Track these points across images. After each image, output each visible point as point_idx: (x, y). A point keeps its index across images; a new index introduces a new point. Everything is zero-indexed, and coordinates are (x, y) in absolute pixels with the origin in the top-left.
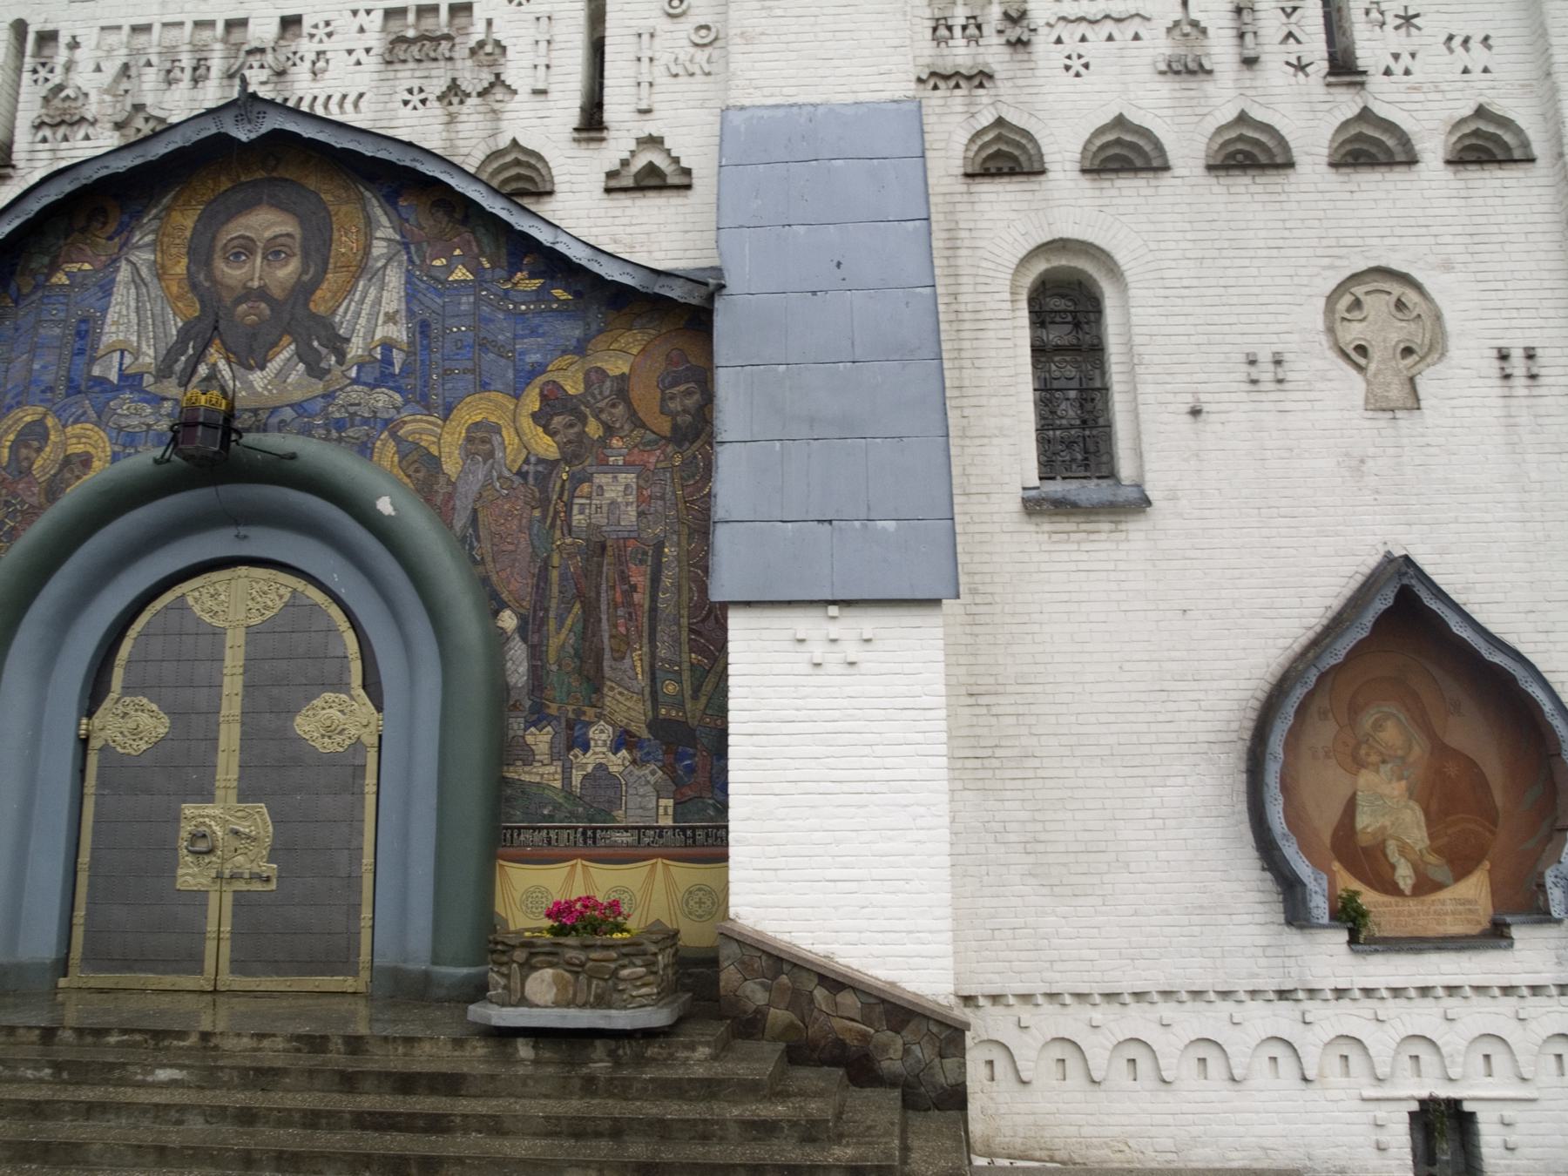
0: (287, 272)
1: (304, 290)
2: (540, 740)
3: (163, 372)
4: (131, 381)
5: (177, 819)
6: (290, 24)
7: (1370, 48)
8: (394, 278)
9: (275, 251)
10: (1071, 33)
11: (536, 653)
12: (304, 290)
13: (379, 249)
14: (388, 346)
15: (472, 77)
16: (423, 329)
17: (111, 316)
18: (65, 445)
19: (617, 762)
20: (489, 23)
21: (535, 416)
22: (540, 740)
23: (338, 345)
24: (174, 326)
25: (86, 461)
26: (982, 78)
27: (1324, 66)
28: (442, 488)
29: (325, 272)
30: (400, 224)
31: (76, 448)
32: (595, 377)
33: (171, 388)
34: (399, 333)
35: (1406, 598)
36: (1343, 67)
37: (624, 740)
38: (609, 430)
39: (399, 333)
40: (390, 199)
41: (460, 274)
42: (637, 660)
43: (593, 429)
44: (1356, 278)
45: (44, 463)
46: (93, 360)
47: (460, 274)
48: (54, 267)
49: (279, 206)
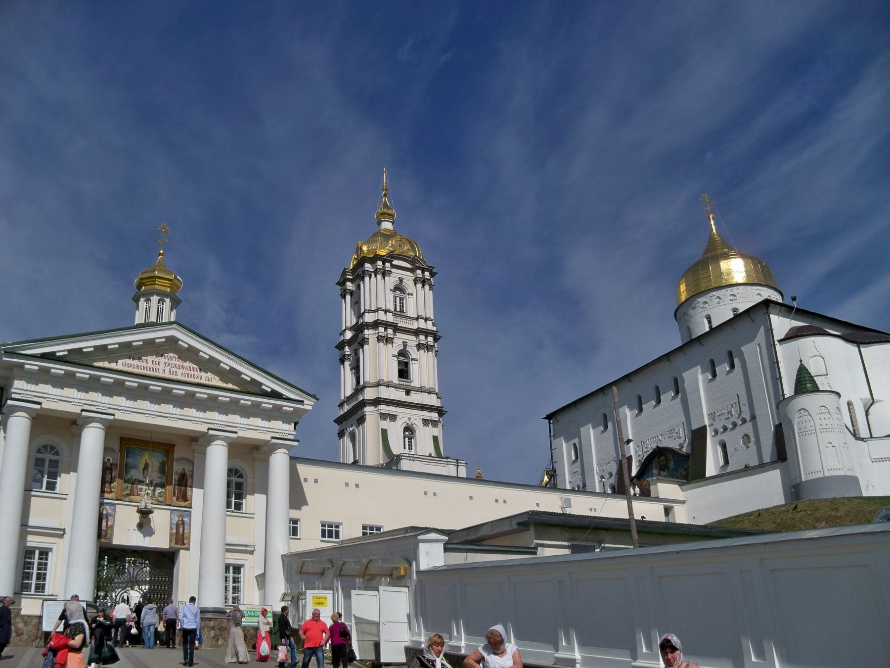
0: (665, 462)
1: (666, 463)
8: (672, 461)
12: (666, 463)
16: (675, 465)
23: (670, 468)
39: (674, 466)
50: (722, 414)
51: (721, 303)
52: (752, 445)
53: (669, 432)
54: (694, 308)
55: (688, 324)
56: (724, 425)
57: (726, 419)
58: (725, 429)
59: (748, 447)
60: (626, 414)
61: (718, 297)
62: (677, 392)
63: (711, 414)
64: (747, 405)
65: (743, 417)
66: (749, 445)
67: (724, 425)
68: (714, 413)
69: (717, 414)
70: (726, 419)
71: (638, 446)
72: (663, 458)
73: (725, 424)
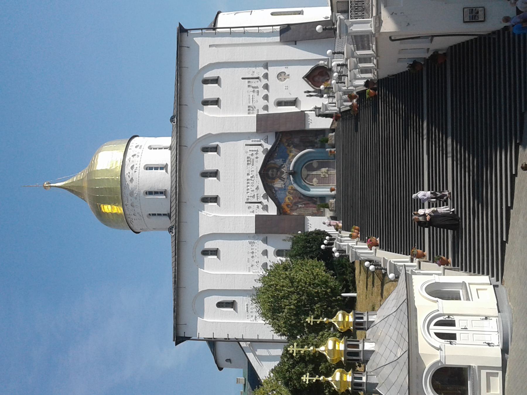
0: (275, 170)
2: (316, 146)
3: (284, 181)
4: (284, 184)
5: (322, 177)
6: (248, 174)
7: (256, 76)
8: (276, 160)
9: (273, 171)
10: (254, 102)
11: (309, 146)
13: (273, 162)
14: (282, 161)
15: (255, 156)
17: (278, 186)
18: (290, 190)
19: (318, 139)
20: (250, 155)
21: (289, 147)
22: (316, 146)
24: (279, 180)
25: (292, 187)
26: (258, 110)
27: (258, 80)
28: (295, 155)
29: (275, 167)
30: (271, 160)
31: (290, 188)
32: (286, 142)
33: (285, 180)
34: (281, 160)
35: (306, 77)
36: (258, 78)
37: (316, 139)
38: (291, 141)
39: (281, 160)
40: (268, 161)
41: (276, 154)
42: (310, 138)
43: (290, 142)
44: (278, 78)
45: (292, 191)
46: (282, 188)
47: (276, 154)
48: (273, 193)
49: (268, 172)
50: (253, 98)
51: (140, 155)
52: (289, 70)
53: (248, 164)
54: (132, 180)
55: (142, 191)
56: (263, 98)
57: (258, 95)
58: (266, 97)
59: (289, 75)
60: (214, 216)
61: (133, 156)
62: (215, 149)
63: (249, 110)
64: (254, 69)
65: (262, 76)
66: (287, 74)
67: (263, 98)
68: (249, 107)
69: (251, 104)
70: (258, 95)
71: (249, 208)
72: (270, 172)
73: (262, 96)
